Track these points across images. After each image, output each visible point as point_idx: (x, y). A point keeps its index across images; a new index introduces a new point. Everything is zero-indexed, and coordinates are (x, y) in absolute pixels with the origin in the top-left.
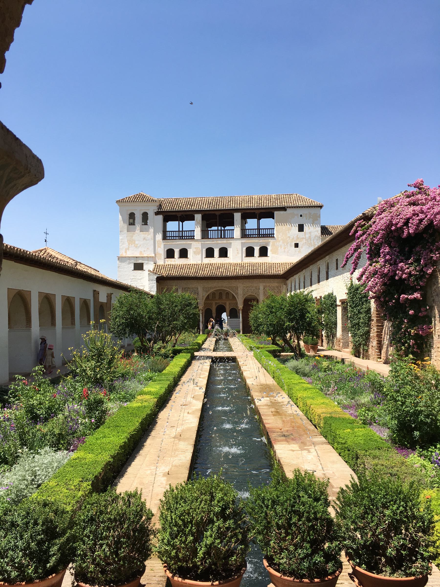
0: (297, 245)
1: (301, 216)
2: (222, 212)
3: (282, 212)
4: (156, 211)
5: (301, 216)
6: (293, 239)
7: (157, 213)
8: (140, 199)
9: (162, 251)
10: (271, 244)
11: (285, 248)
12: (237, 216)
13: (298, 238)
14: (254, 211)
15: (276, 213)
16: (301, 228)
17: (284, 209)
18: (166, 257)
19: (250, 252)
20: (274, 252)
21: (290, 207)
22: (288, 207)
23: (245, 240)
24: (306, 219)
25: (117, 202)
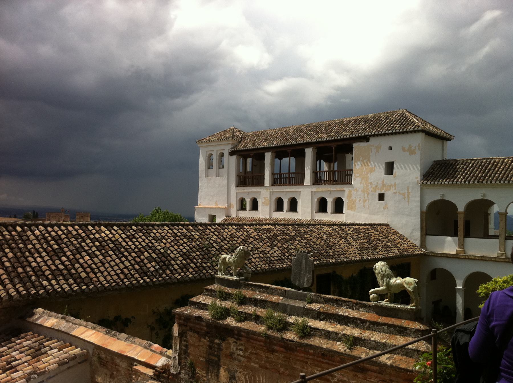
0: (381, 197)
3: (363, 145)
6: (376, 186)
7: (232, 153)
9: (234, 202)
10: (346, 193)
11: (365, 201)
13: (383, 185)
14: (327, 145)
15: (355, 145)
16: (390, 168)
17: (366, 139)
18: (238, 208)
19: (322, 206)
20: (350, 208)
21: (374, 136)
22: (370, 136)
23: (315, 188)
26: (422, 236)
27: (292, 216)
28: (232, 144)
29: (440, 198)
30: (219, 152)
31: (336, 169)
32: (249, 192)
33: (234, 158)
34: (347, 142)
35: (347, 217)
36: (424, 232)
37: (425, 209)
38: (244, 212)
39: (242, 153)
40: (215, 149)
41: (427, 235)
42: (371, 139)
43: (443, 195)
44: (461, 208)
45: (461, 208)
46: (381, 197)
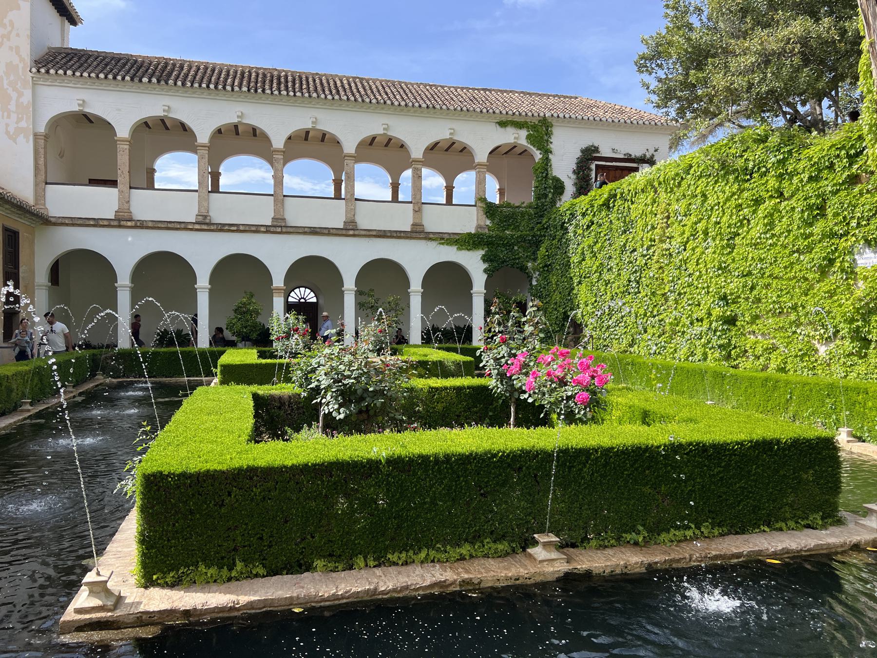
26: (36, 185)
29: (76, 108)
36: (42, 177)
37: (42, 129)
41: (47, 183)
43: (84, 101)
44: (123, 131)
45: (123, 131)
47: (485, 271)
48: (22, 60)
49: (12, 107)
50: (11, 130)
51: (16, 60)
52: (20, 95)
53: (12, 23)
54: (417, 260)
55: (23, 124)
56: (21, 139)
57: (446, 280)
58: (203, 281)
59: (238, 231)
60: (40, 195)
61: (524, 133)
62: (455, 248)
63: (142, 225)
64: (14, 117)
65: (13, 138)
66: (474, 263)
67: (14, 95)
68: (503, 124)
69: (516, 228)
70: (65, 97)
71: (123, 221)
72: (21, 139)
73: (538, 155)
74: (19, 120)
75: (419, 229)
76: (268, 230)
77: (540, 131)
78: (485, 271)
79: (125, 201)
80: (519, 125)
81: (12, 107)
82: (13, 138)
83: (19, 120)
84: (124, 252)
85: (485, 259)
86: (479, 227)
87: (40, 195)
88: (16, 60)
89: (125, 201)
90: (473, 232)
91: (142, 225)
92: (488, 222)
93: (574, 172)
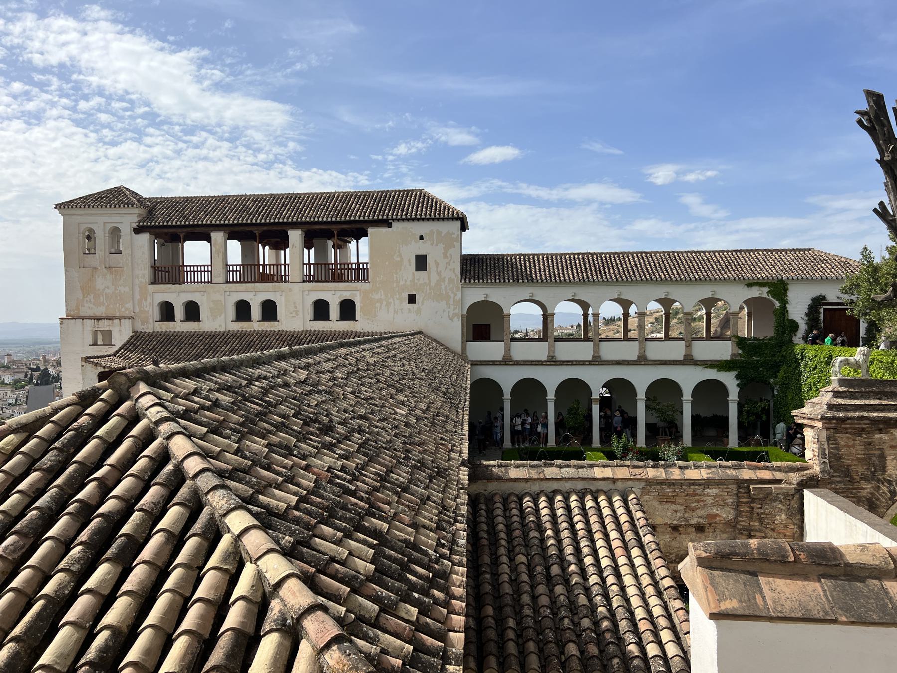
0: (412, 299)
1: (421, 238)
2: (265, 228)
3: (383, 230)
4: (135, 226)
5: (421, 238)
7: (138, 230)
8: (116, 198)
12: (295, 236)
16: (421, 263)
17: (387, 223)
24: (432, 244)
25: (59, 207)
27: (268, 326)
28: (139, 215)
29: (483, 299)
30: (109, 227)
31: (313, 261)
32: (177, 296)
33: (145, 238)
34: (358, 226)
35: (362, 324)
36: (465, 339)
37: (465, 312)
38: (171, 323)
39: (157, 231)
40: (101, 220)
42: (394, 224)
46: (412, 299)
47: (738, 385)
48: (456, 275)
49: (451, 302)
50: (451, 314)
51: (453, 277)
52: (455, 295)
53: (451, 256)
54: (688, 380)
55: (457, 311)
56: (456, 319)
57: (709, 391)
58: (551, 396)
59: (572, 361)
60: (464, 349)
61: (766, 289)
62: (715, 370)
63: (518, 363)
64: (452, 307)
65: (452, 319)
66: (729, 380)
67: (452, 295)
68: (750, 285)
69: (761, 355)
70: (477, 294)
71: (507, 361)
72: (456, 319)
73: (777, 304)
74: (455, 309)
75: (689, 358)
76: (590, 363)
77: (779, 288)
78: (738, 385)
79: (508, 349)
80: (761, 284)
81: (451, 302)
82: (452, 319)
83: (455, 309)
84: (507, 379)
85: (737, 377)
86: (733, 355)
87: (464, 349)
88: (453, 277)
89: (508, 349)
90: (728, 358)
91: (518, 363)
92: (740, 352)
93: (806, 314)
